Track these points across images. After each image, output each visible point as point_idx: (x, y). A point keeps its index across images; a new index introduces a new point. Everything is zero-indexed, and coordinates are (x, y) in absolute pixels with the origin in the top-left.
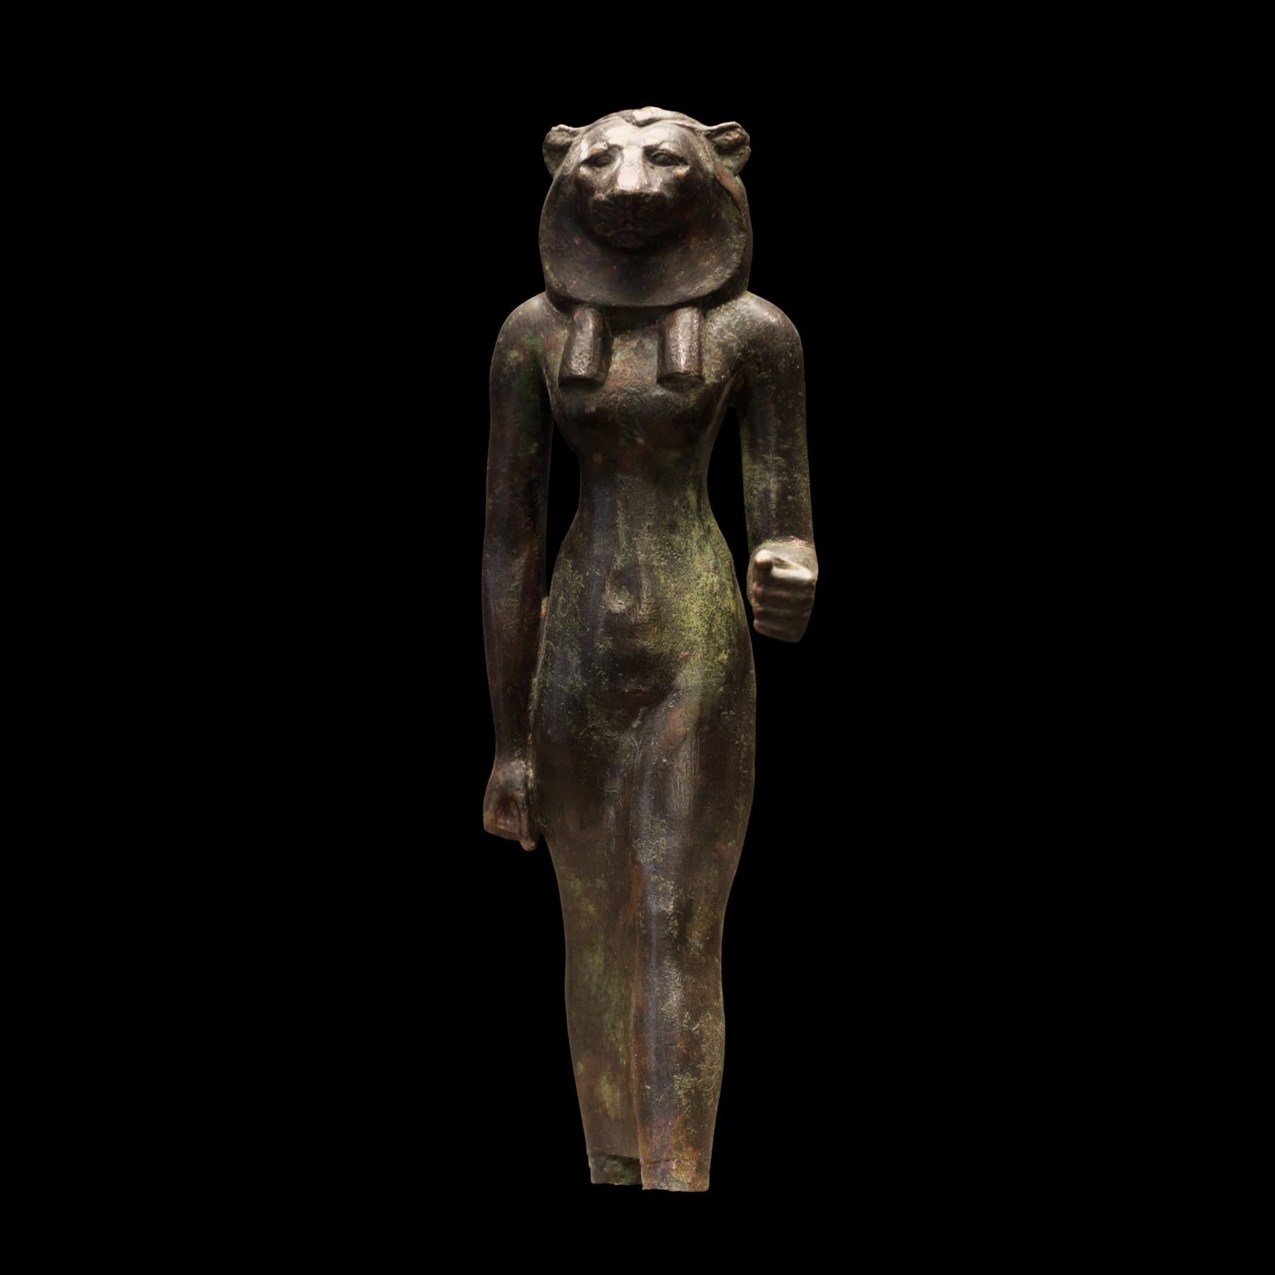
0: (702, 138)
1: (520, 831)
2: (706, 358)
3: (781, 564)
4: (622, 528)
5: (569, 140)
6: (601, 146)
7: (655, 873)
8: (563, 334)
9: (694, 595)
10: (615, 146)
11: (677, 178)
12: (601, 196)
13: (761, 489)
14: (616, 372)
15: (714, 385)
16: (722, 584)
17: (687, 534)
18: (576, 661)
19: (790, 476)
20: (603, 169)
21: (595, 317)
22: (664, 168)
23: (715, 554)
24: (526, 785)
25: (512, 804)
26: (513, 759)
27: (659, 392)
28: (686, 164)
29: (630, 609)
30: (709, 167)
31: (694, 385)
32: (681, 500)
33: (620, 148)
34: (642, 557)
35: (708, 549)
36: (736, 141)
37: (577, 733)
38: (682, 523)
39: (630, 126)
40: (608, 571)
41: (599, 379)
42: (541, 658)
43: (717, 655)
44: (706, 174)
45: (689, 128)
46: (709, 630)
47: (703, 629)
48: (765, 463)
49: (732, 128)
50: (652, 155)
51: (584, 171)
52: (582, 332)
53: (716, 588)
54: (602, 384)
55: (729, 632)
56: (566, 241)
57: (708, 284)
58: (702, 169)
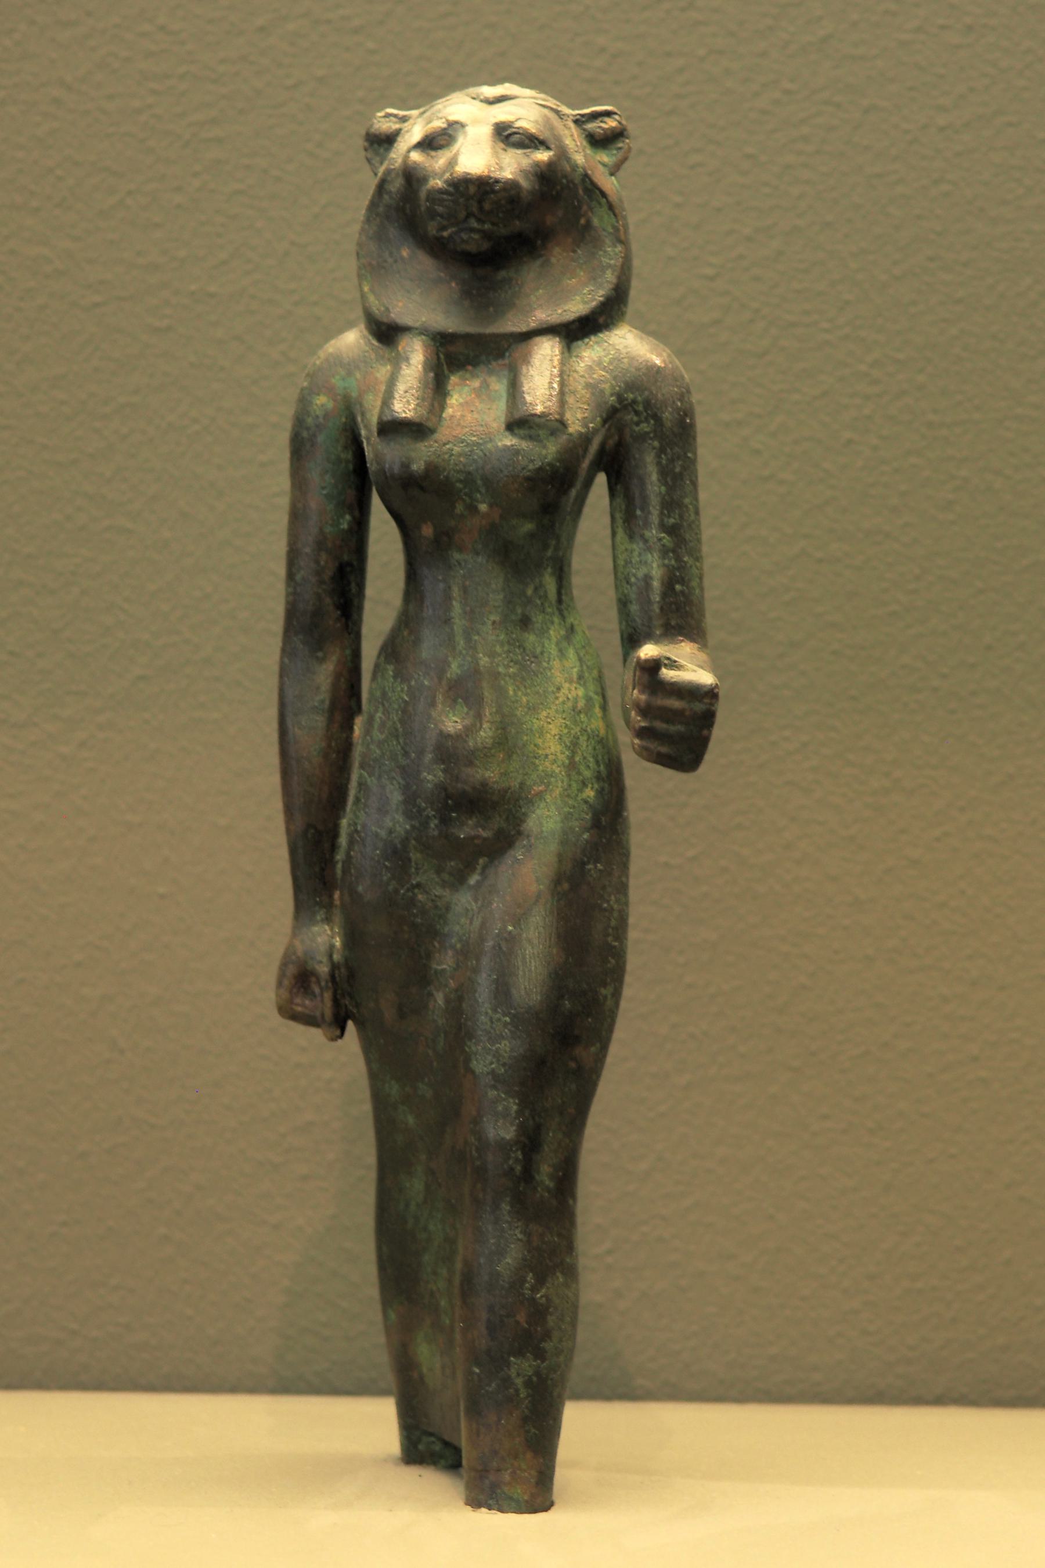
0: (572, 125)
1: (323, 1015)
2: (570, 400)
3: (673, 665)
4: (459, 624)
5: (397, 126)
6: (439, 124)
7: (494, 1087)
8: (383, 372)
9: (552, 713)
10: (457, 122)
11: (537, 164)
12: (438, 183)
13: (640, 574)
14: (452, 417)
15: (581, 434)
16: (589, 700)
17: (543, 632)
18: (396, 797)
19: (678, 559)
20: (440, 152)
21: (426, 346)
22: (519, 151)
23: (580, 660)
24: (331, 956)
25: (313, 979)
26: (314, 922)
27: (509, 441)
28: (548, 148)
29: (469, 730)
30: (579, 159)
31: (553, 433)
32: (536, 589)
33: (463, 126)
34: (484, 661)
35: (571, 653)
36: (613, 129)
37: (396, 891)
38: (538, 619)
39: (477, 103)
40: (440, 679)
41: (430, 424)
42: (352, 793)
43: (580, 791)
44: (575, 167)
45: (552, 109)
46: (571, 758)
47: (561, 757)
48: (646, 541)
49: (608, 114)
50: (506, 135)
51: (416, 156)
52: (409, 365)
53: (581, 704)
54: (432, 431)
55: (597, 762)
56: (391, 254)
57: (576, 307)
58: (568, 159)
